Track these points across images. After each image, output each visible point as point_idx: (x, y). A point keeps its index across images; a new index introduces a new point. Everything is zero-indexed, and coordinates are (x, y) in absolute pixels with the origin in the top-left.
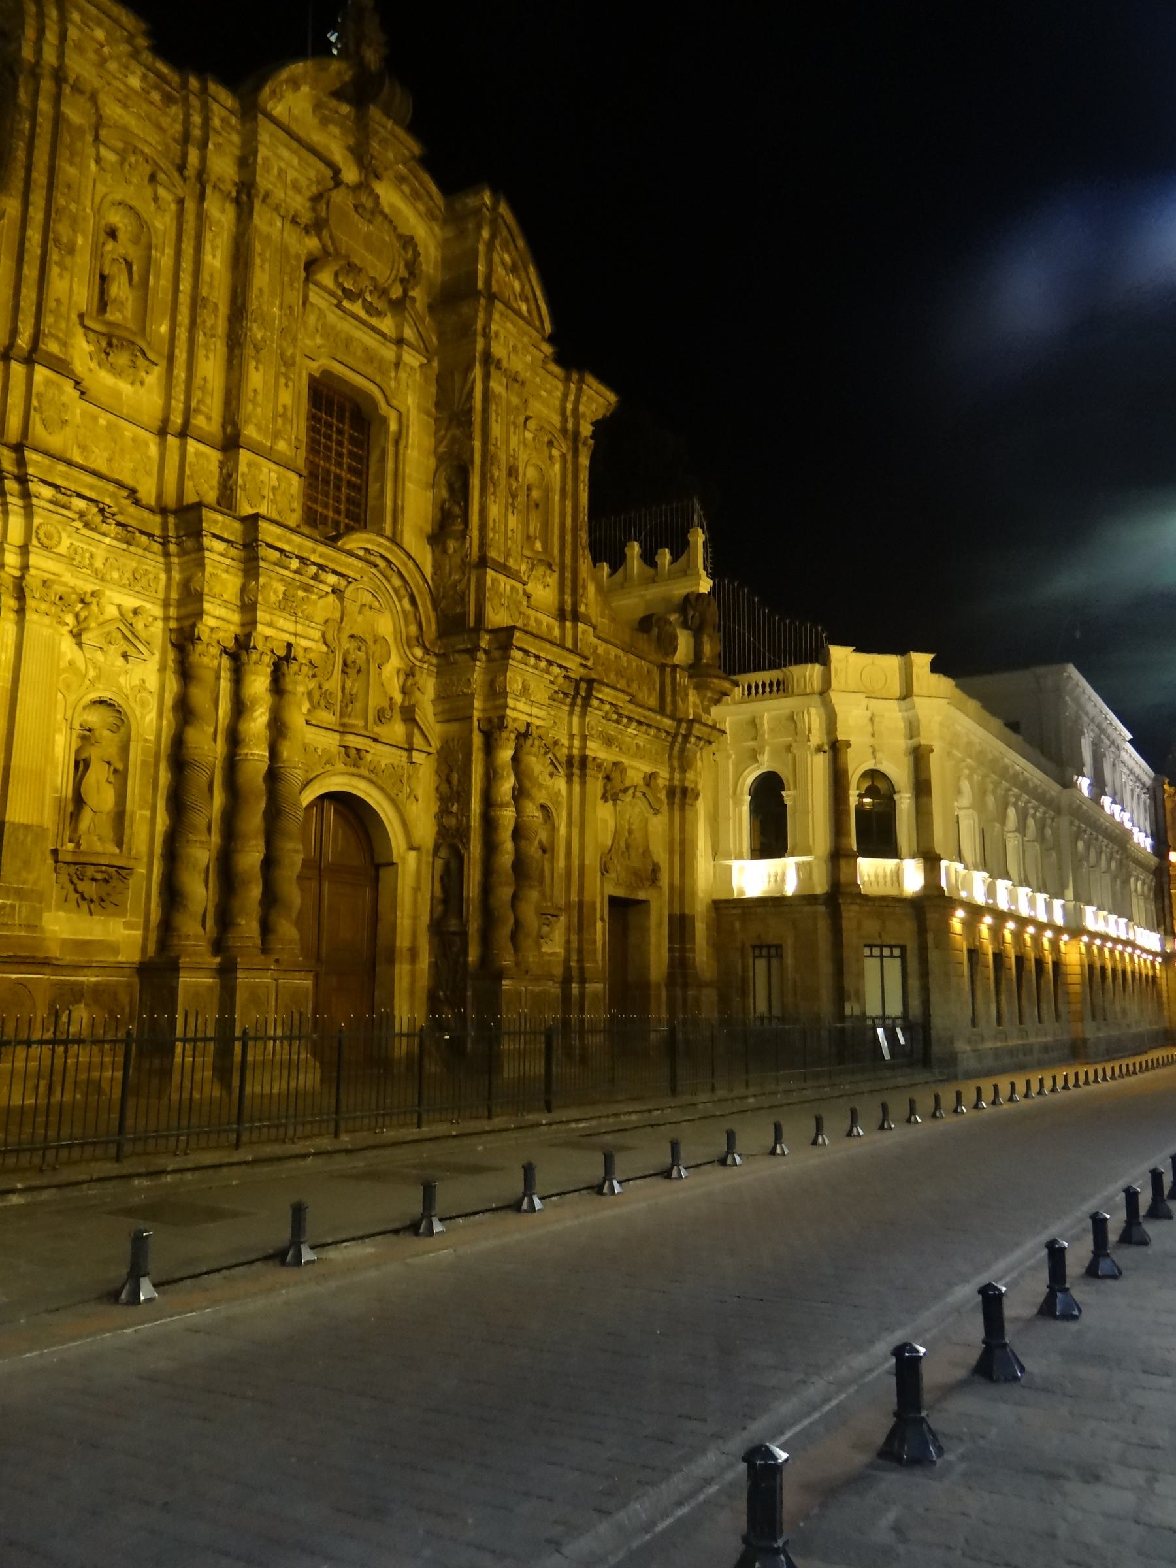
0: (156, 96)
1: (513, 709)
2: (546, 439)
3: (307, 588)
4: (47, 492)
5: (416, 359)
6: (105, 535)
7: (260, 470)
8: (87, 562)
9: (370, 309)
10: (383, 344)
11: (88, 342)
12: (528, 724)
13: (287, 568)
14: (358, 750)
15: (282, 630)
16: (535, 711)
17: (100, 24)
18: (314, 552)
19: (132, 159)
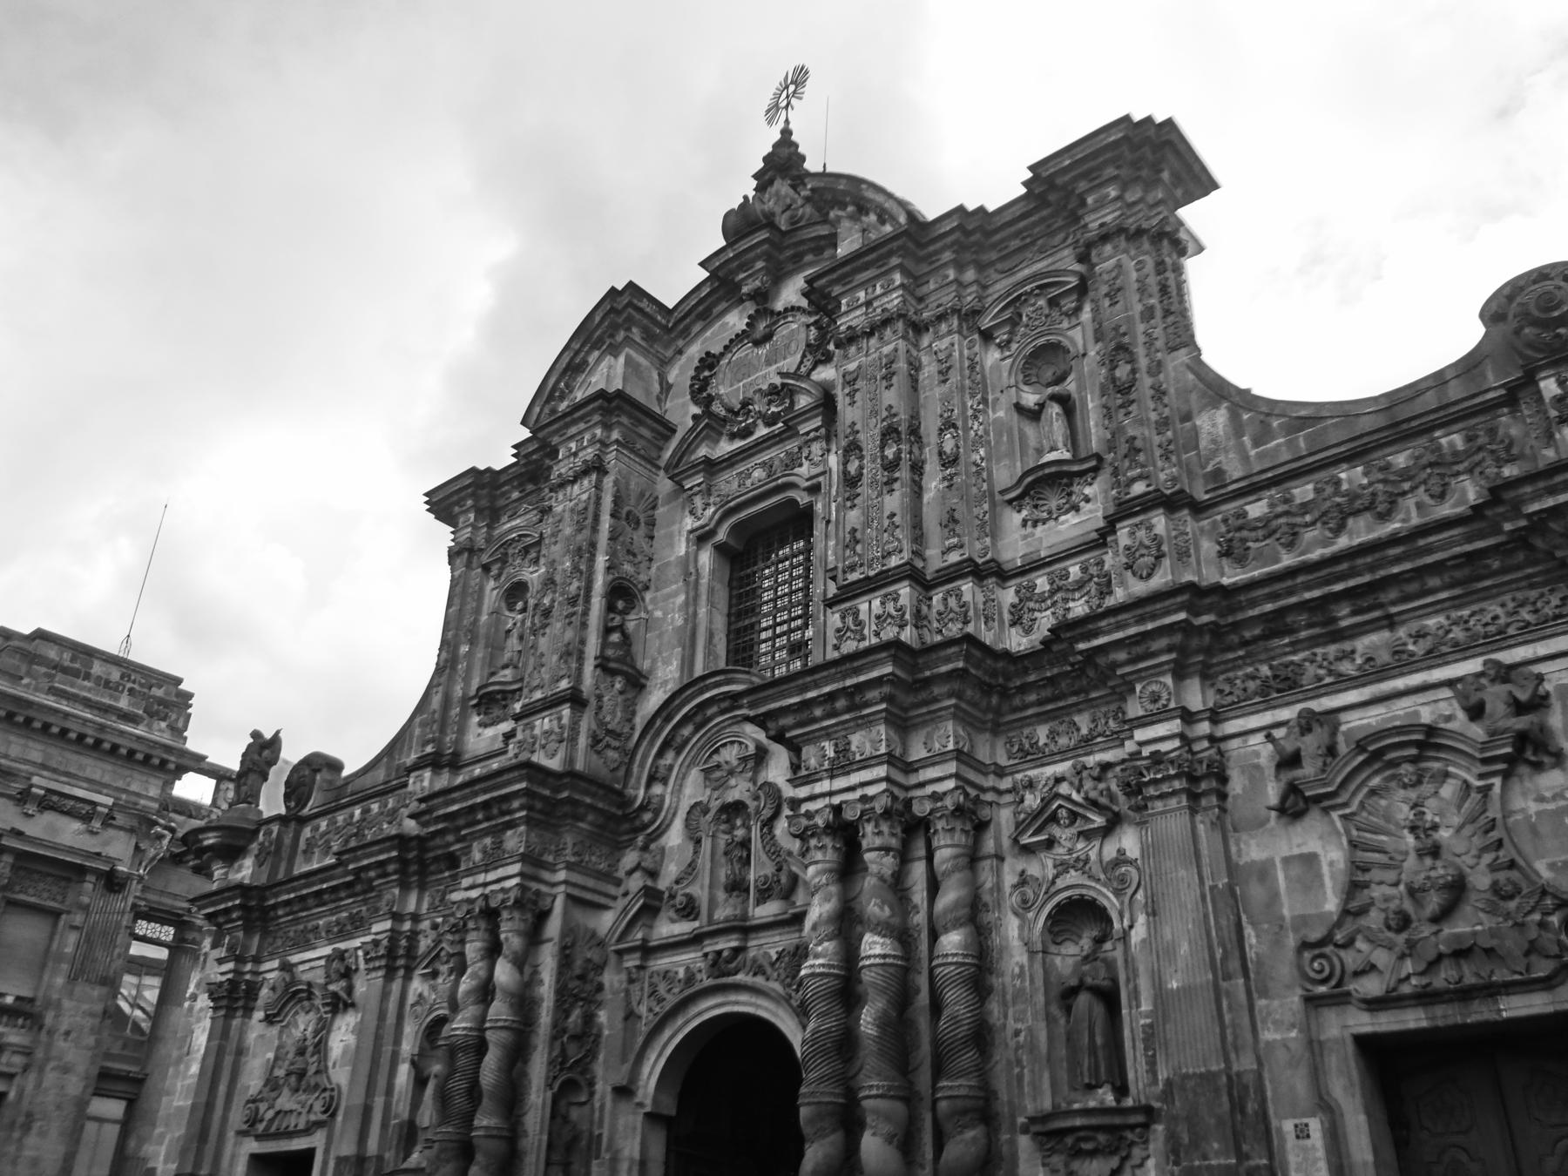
0: (530, 487)
1: (812, 798)
2: (1042, 302)
3: (511, 825)
4: (372, 874)
5: (816, 416)
6: (442, 872)
7: (533, 728)
8: (437, 903)
9: (770, 421)
10: (781, 441)
11: (479, 714)
12: (837, 810)
13: (480, 822)
14: (719, 953)
15: (485, 885)
16: (855, 778)
17: (464, 499)
18: (476, 794)
19: (511, 551)
